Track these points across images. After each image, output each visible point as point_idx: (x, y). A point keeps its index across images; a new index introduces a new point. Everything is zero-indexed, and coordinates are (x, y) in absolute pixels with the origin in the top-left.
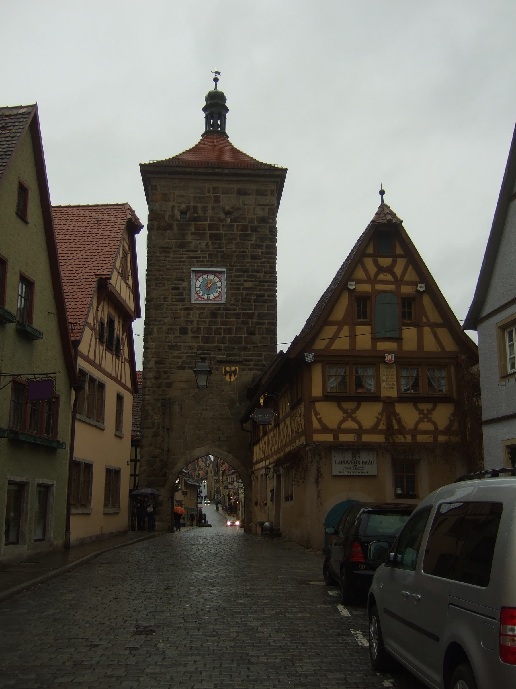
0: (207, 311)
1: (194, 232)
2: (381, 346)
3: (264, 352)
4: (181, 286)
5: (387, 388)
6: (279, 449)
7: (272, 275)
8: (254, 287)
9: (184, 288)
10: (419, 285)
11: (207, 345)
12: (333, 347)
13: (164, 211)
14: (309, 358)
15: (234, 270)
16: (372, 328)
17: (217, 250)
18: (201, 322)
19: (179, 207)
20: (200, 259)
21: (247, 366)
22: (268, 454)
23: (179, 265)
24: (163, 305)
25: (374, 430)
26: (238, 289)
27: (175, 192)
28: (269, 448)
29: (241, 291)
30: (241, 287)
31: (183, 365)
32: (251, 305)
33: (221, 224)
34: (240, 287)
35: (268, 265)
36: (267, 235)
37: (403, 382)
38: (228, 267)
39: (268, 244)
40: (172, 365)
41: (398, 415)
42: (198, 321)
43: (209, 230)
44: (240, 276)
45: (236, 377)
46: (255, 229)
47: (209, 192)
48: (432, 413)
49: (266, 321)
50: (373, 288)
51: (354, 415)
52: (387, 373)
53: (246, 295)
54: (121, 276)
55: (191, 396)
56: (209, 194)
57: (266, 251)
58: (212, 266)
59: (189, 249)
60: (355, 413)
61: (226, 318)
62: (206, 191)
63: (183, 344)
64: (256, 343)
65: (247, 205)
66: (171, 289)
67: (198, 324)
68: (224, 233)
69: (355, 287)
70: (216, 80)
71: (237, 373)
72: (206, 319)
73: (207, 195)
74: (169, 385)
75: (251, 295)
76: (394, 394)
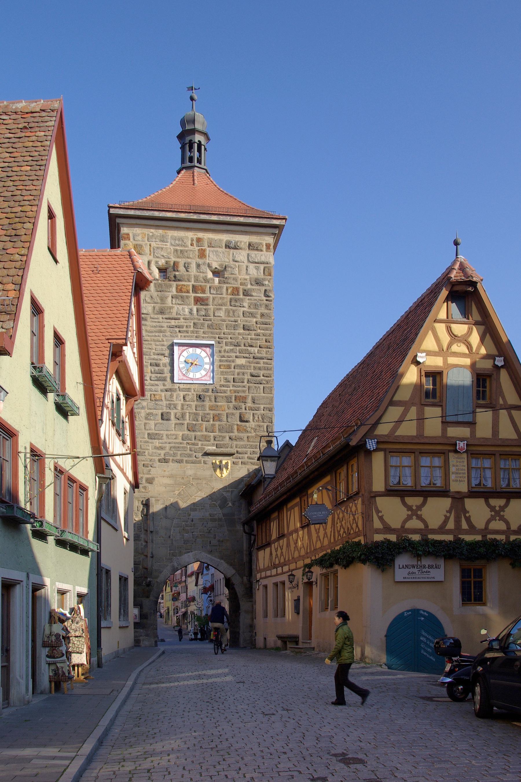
0: (193, 392)
4: (161, 363)
5: (456, 481)
8: (248, 364)
9: (165, 365)
18: (186, 406)
26: (229, 367)
34: (230, 363)
35: (264, 338)
41: (468, 512)
42: (182, 405)
44: (232, 351)
51: (419, 513)
52: (457, 464)
57: (262, 320)
63: (165, 433)
67: (182, 409)
71: (229, 467)
72: (192, 403)
76: (463, 488)
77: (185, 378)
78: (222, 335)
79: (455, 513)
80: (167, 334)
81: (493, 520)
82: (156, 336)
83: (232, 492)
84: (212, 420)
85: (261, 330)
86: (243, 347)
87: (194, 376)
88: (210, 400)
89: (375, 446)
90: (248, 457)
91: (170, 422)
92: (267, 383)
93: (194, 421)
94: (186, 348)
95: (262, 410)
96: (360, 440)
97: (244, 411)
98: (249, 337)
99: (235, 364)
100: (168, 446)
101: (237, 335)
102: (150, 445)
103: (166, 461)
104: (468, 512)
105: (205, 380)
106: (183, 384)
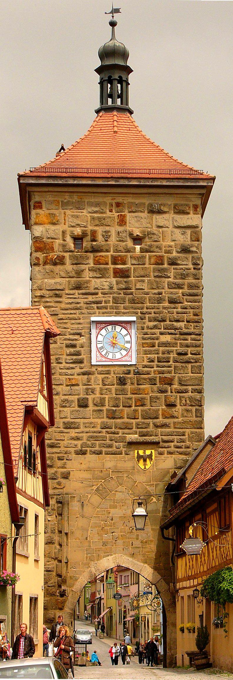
0: (112, 375)
1: (93, 267)
3: (188, 429)
15: (147, 318)
17: (125, 291)
19: (72, 232)
20: (101, 303)
22: (196, 572)
26: (154, 346)
27: (64, 210)
28: (197, 564)
30: (157, 342)
31: (83, 449)
34: (154, 341)
36: (190, 269)
38: (139, 314)
42: (101, 389)
44: (155, 327)
45: (152, 463)
46: (173, 263)
47: (111, 211)
53: (163, 353)
55: (95, 489)
58: (117, 314)
59: (88, 291)
61: (138, 385)
63: (82, 420)
64: (177, 418)
68: (132, 267)
70: (113, 24)
71: (153, 458)
75: (169, 352)
77: (104, 359)
78: (145, 310)
80: (83, 311)
82: (71, 314)
83: (156, 485)
85: (188, 302)
86: (168, 322)
87: (114, 357)
90: (174, 446)
91: (88, 409)
92: (196, 362)
93: (114, 406)
95: (190, 392)
96: (226, 485)
97: (169, 393)
99: (159, 341)
103: (84, 453)
106: (101, 366)
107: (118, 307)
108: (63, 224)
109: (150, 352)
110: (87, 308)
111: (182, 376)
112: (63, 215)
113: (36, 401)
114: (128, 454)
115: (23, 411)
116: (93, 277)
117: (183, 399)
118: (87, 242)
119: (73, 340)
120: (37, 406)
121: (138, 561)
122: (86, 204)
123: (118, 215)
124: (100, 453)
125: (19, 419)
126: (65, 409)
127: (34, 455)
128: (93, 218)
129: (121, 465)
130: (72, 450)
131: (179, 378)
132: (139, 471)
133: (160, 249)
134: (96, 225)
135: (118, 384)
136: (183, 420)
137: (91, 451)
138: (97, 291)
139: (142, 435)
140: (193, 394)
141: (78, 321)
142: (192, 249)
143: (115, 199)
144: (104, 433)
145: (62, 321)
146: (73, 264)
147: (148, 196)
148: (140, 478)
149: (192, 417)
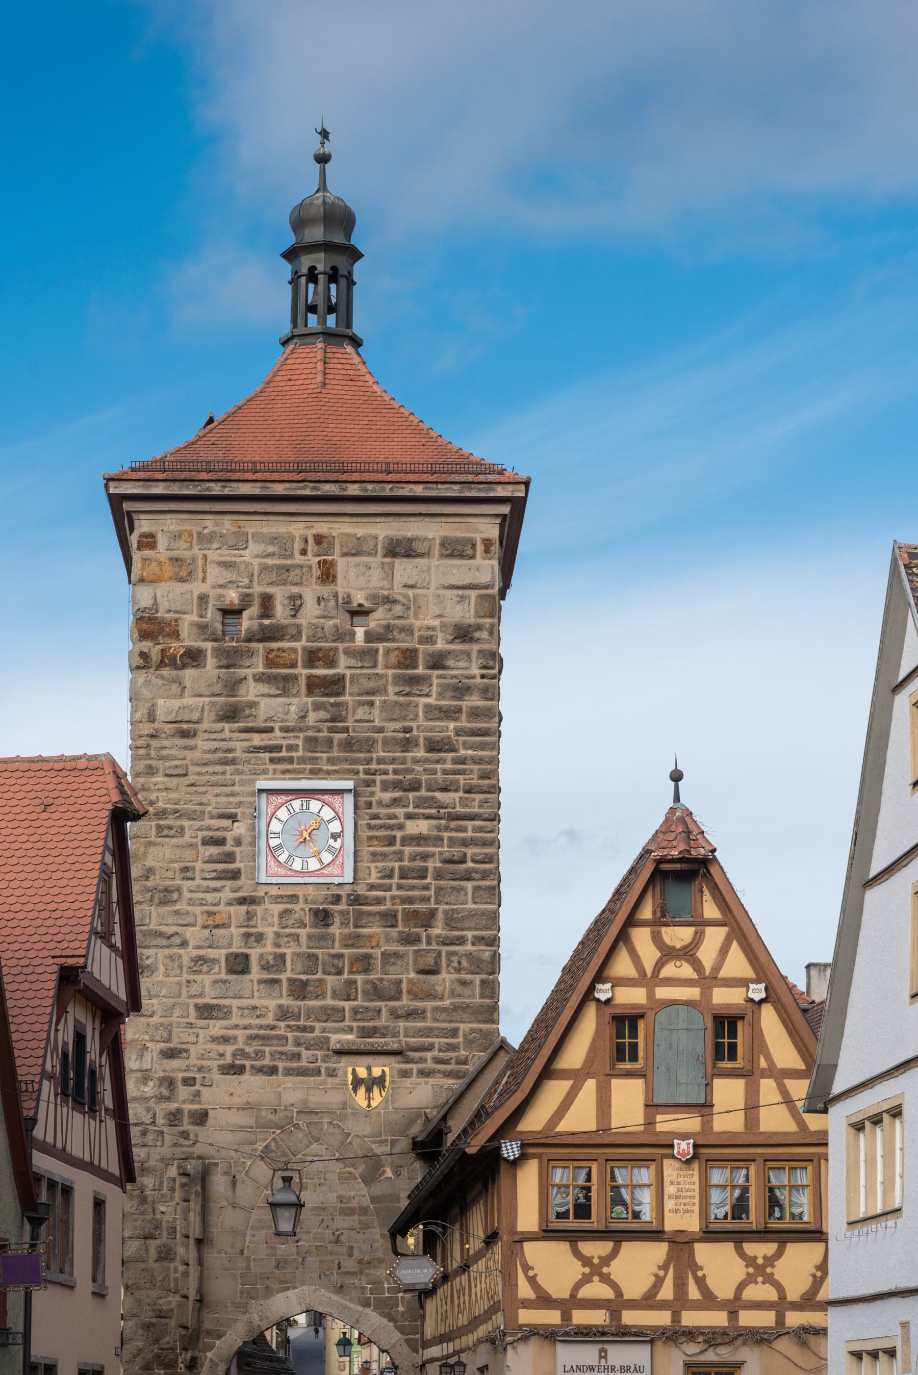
1: (263, 674)
2: (665, 1123)
3: (464, 1022)
4: (229, 836)
5: (677, 1211)
6: (470, 1322)
7: (488, 796)
8: (435, 833)
9: (238, 842)
10: (752, 986)
11: (302, 1003)
12: (561, 1127)
13: (177, 612)
14: (510, 1150)
16: (646, 1083)
20: (280, 751)
21: (416, 1063)
23: (223, 773)
24: (178, 889)
25: (649, 1301)
26: (391, 841)
29: (398, 847)
30: (399, 835)
31: (238, 1062)
32: (426, 888)
33: (341, 646)
34: (393, 833)
35: (476, 767)
36: (473, 677)
37: (716, 1196)
38: (362, 776)
39: (473, 704)
40: (205, 1063)
41: (701, 1269)
42: (277, 935)
43: (305, 666)
44: (395, 802)
45: (384, 1094)
47: (304, 552)
48: (776, 1263)
49: (469, 934)
50: (651, 995)
51: (605, 1270)
52: (680, 1180)
53: (413, 858)
54: (101, 937)
55: (261, 1148)
56: (302, 557)
58: (315, 773)
59: (250, 725)
60: (609, 1266)
61: (356, 926)
62: (297, 546)
63: (235, 1003)
64: (442, 998)
65: (412, 587)
66: (199, 844)
68: (348, 673)
69: (609, 995)
71: (387, 1084)
73: (299, 559)
74: (201, 1118)
75: (425, 857)
76: (693, 1224)
77: (283, 872)
78: (374, 766)
79: (675, 1271)
80: (240, 767)
81: (750, 1282)
82: (214, 773)
84: (346, 969)
85: (466, 749)
88: (344, 924)
89: (516, 1153)
91: (247, 977)
92: (483, 878)
93: (304, 973)
94: (284, 798)
95: (469, 942)
98: (439, 766)
100: (241, 1034)
101: (409, 765)
102: (201, 1032)
103: (241, 1070)
104: (701, 1269)
105: (332, 875)
106: (277, 887)
107: (317, 758)
108: (200, 581)
109: (384, 856)
110: (248, 762)
111: (453, 910)
112: (200, 562)
113: (83, 956)
114: (332, 1076)
115: (54, 977)
116: (263, 695)
117: (455, 959)
118: (251, 619)
119: (218, 830)
120: (85, 967)
121: (351, 1300)
122: (250, 539)
123: (319, 562)
124: (273, 1071)
125: (46, 993)
126: (198, 978)
127: (93, 1072)
128: (264, 568)
129: (317, 1099)
130: (214, 1064)
131: (446, 912)
132: (356, 1112)
133: (412, 634)
134: (271, 584)
135: (312, 927)
136: (452, 1004)
137: (252, 1067)
138: (270, 725)
139: (366, 1033)
140: (475, 948)
141: (228, 790)
142: (477, 635)
143: (312, 527)
144: (283, 1029)
145: (193, 789)
146: (219, 667)
147: (383, 519)
148: (358, 1127)
149: (473, 996)
